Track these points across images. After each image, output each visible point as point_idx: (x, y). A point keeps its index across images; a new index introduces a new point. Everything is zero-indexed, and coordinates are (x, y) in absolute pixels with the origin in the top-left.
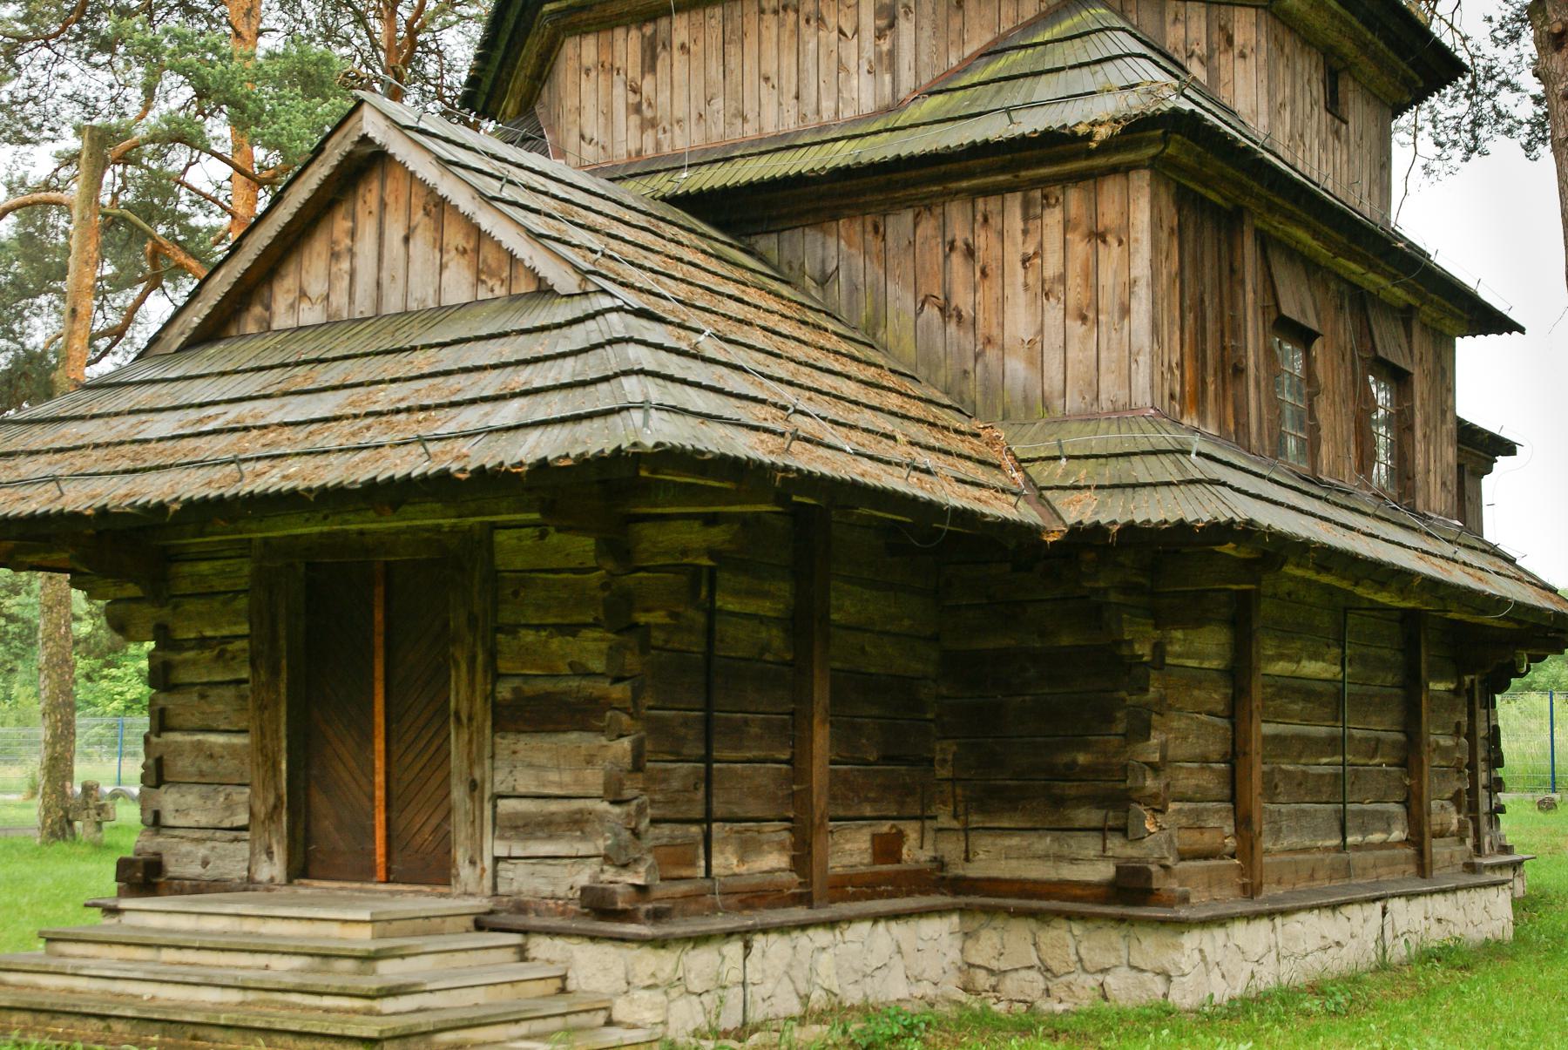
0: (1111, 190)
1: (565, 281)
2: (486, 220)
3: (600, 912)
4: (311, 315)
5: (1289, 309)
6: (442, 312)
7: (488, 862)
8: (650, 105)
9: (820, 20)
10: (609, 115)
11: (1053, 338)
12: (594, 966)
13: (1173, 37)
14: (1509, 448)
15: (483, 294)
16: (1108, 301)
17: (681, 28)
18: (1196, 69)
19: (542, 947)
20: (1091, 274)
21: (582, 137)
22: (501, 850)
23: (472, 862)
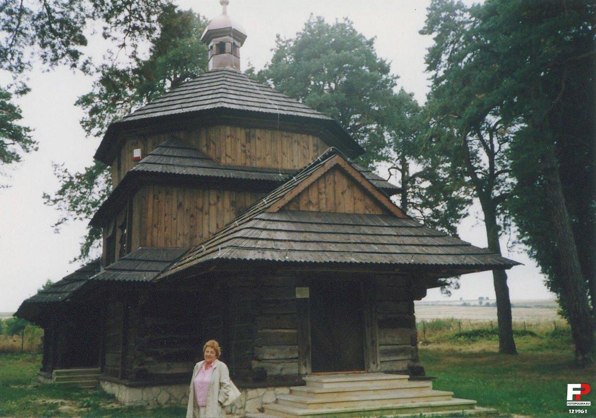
7: (379, 362)
8: (249, 151)
15: (367, 212)
21: (227, 155)
22: (382, 359)
23: (374, 363)
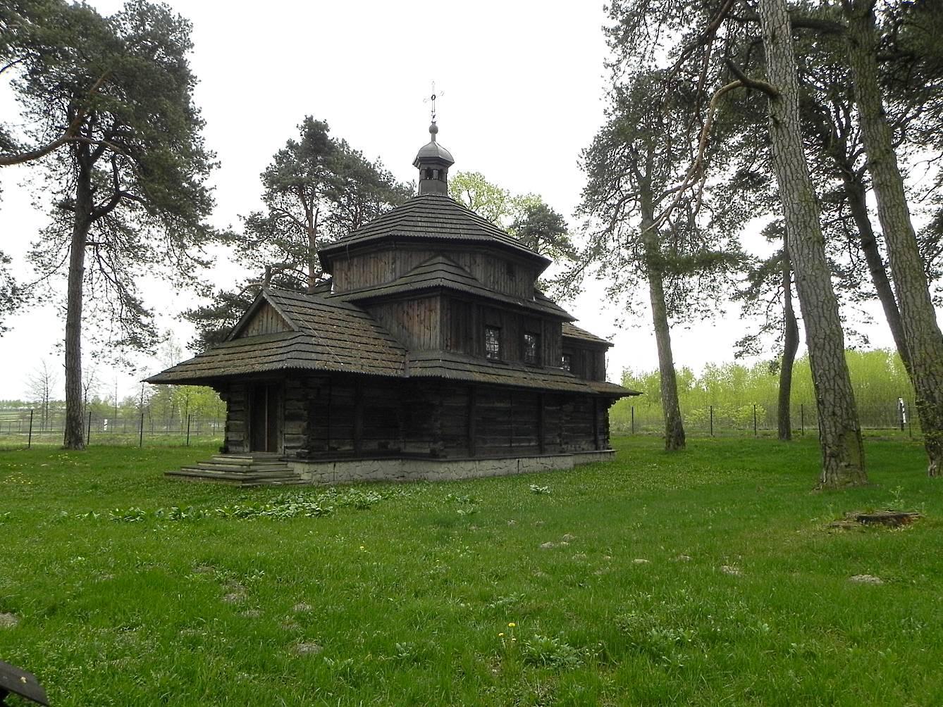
0: (433, 301)
1: (296, 329)
3: (300, 458)
4: (255, 333)
9: (381, 260)
10: (341, 279)
12: (298, 468)
13: (461, 263)
14: (612, 345)
18: (467, 269)
19: (290, 465)
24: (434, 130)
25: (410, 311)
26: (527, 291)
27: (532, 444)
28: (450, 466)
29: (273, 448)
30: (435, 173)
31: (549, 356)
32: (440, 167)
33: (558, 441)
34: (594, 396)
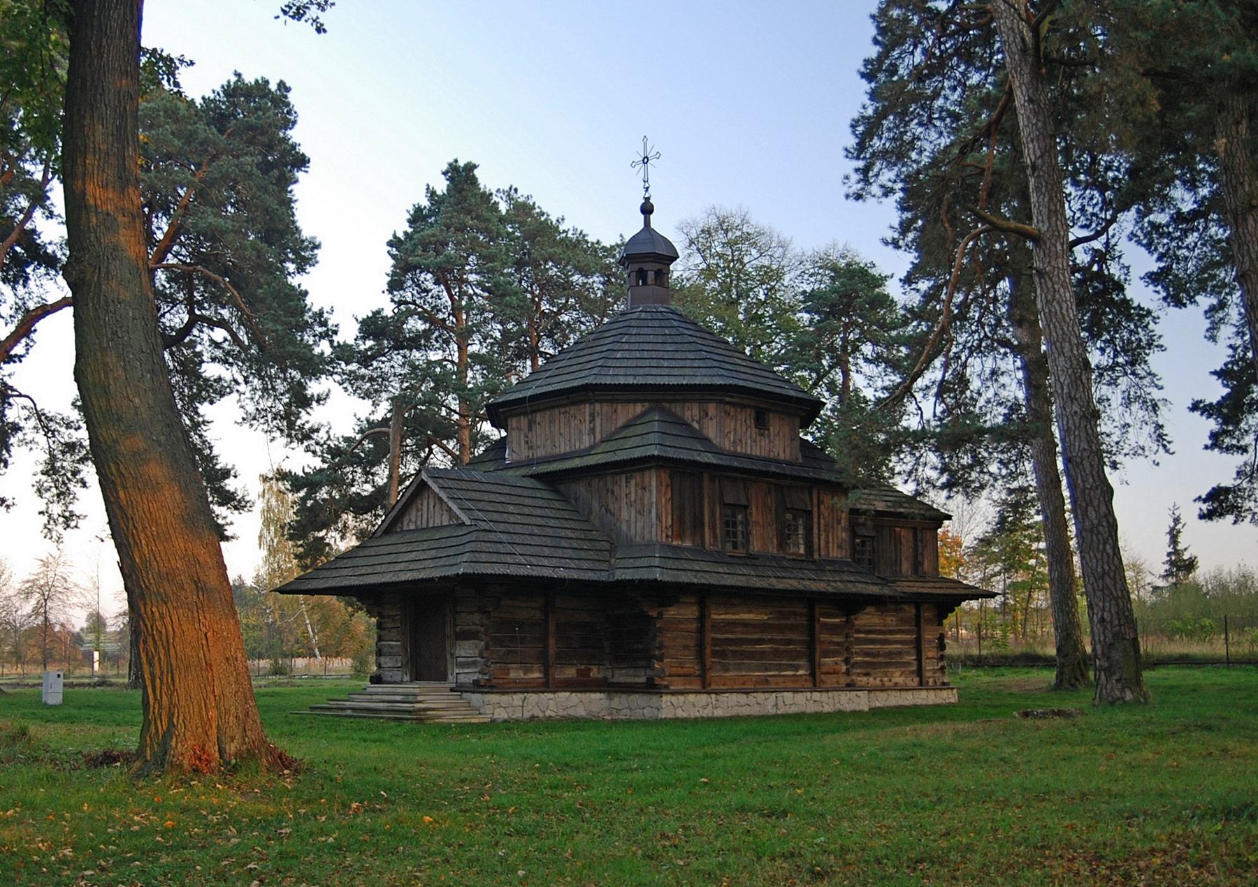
0: (647, 473)
1: (468, 522)
2: (451, 504)
3: (477, 687)
4: (412, 527)
5: (729, 499)
6: (442, 527)
11: (633, 519)
12: (476, 698)
16: (646, 509)
17: (539, 417)
18: (696, 425)
19: (465, 695)
20: (642, 499)
24: (647, 209)
25: (616, 489)
26: (788, 449)
27: (800, 672)
28: (674, 699)
29: (443, 678)
30: (651, 275)
31: (827, 542)
32: (657, 266)
33: (844, 668)
34: (918, 600)
